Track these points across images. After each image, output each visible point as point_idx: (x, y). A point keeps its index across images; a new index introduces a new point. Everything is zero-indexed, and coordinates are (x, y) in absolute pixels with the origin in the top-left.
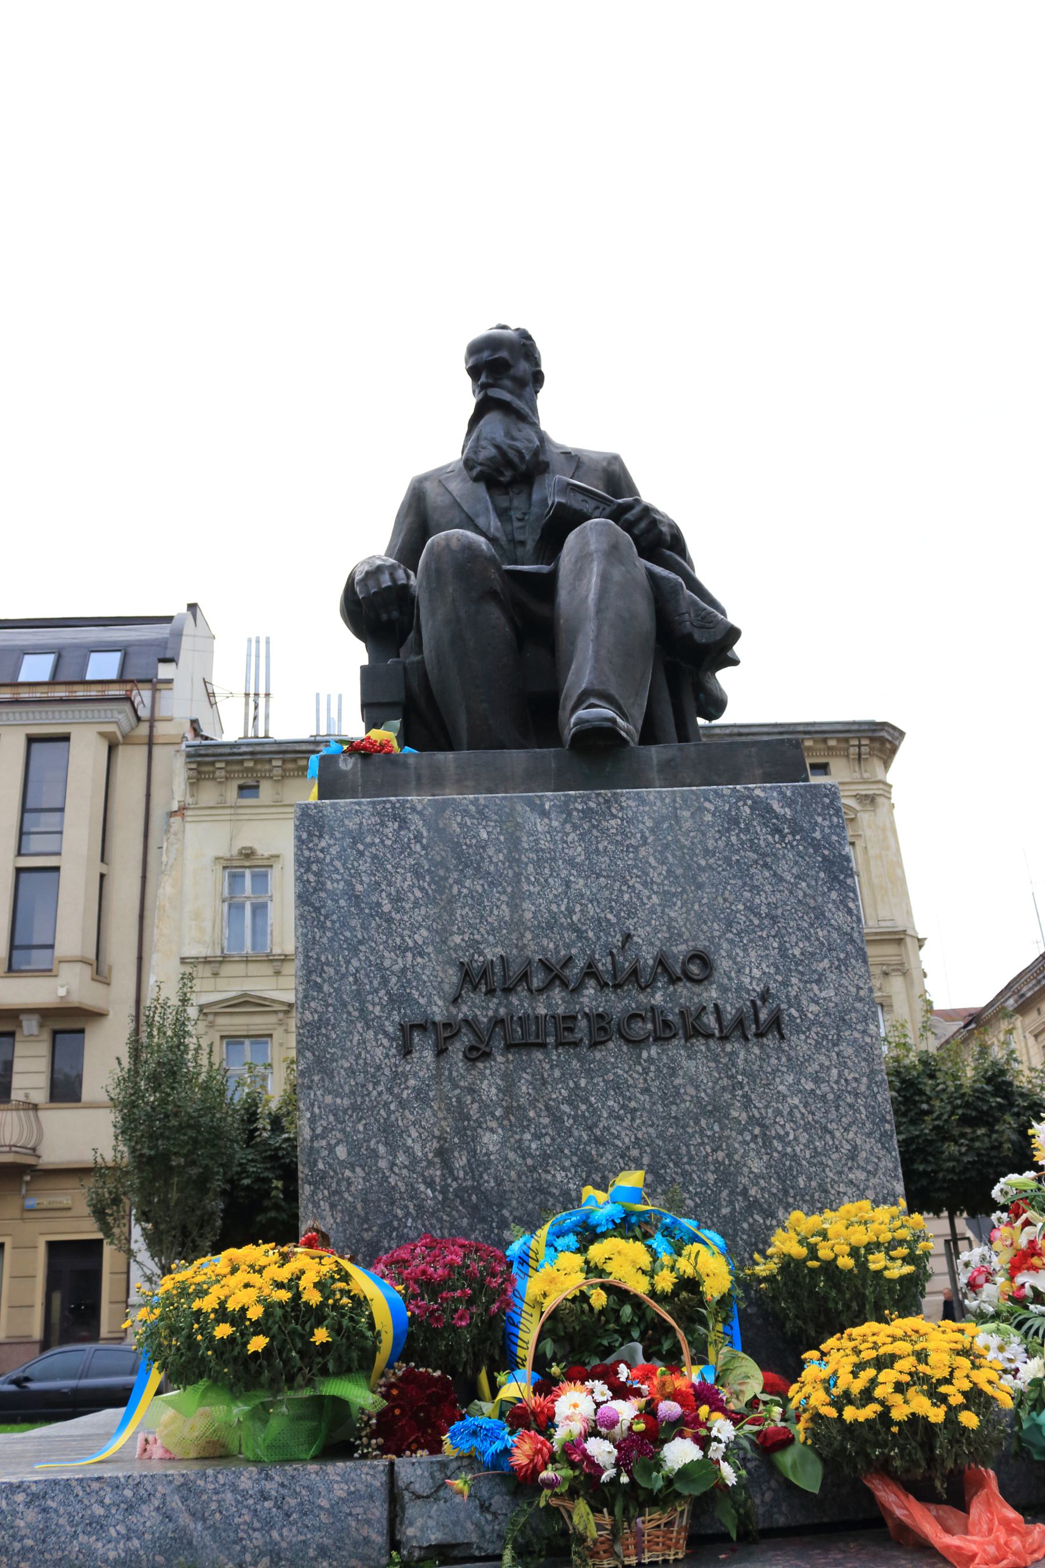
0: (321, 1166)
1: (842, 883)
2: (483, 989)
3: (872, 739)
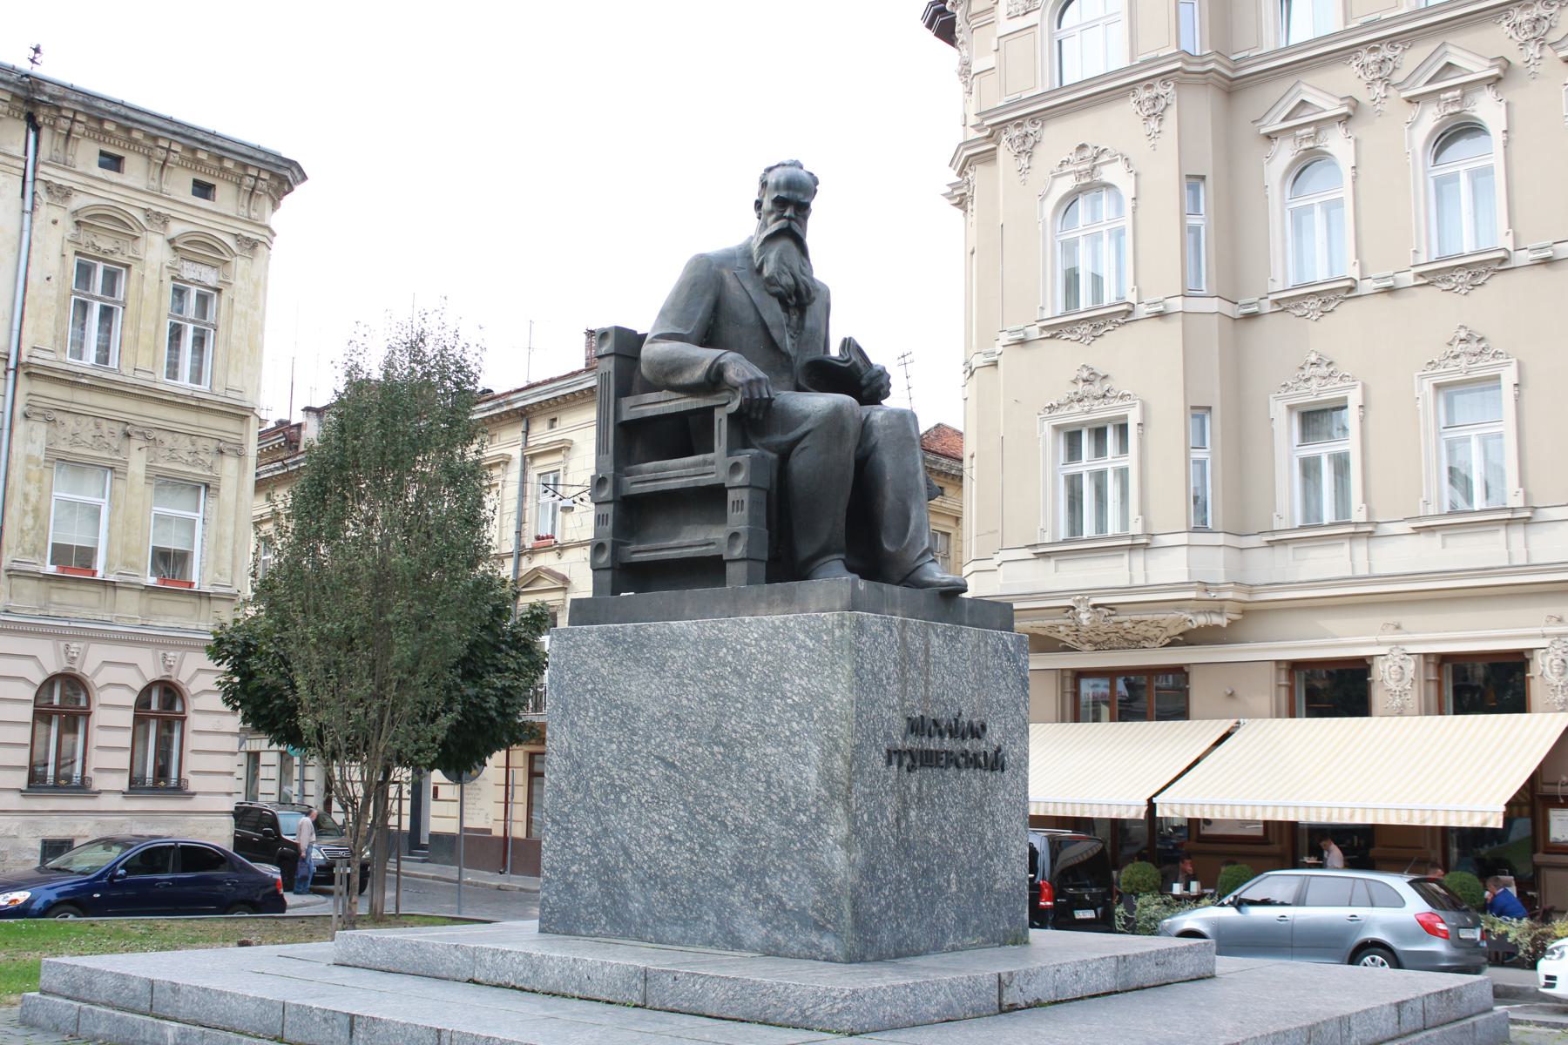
3: (273, 175)
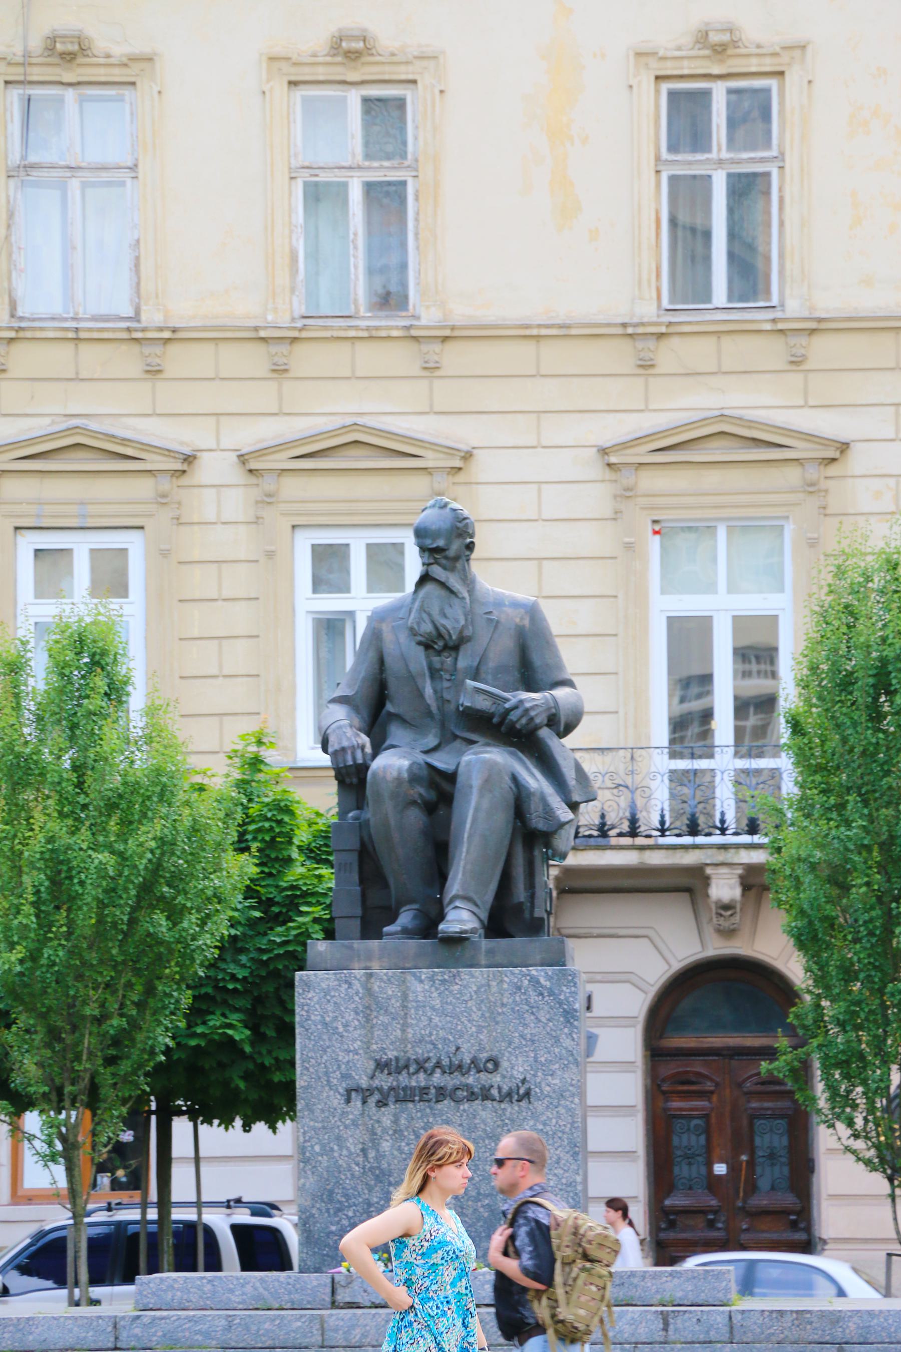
0: (308, 1154)
1: (571, 1024)
2: (386, 1072)
